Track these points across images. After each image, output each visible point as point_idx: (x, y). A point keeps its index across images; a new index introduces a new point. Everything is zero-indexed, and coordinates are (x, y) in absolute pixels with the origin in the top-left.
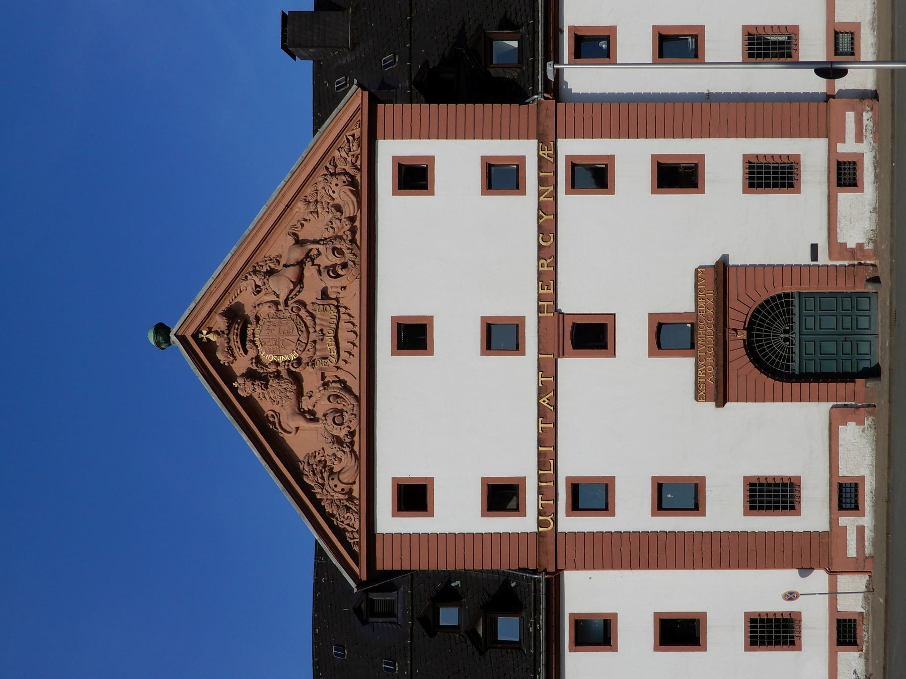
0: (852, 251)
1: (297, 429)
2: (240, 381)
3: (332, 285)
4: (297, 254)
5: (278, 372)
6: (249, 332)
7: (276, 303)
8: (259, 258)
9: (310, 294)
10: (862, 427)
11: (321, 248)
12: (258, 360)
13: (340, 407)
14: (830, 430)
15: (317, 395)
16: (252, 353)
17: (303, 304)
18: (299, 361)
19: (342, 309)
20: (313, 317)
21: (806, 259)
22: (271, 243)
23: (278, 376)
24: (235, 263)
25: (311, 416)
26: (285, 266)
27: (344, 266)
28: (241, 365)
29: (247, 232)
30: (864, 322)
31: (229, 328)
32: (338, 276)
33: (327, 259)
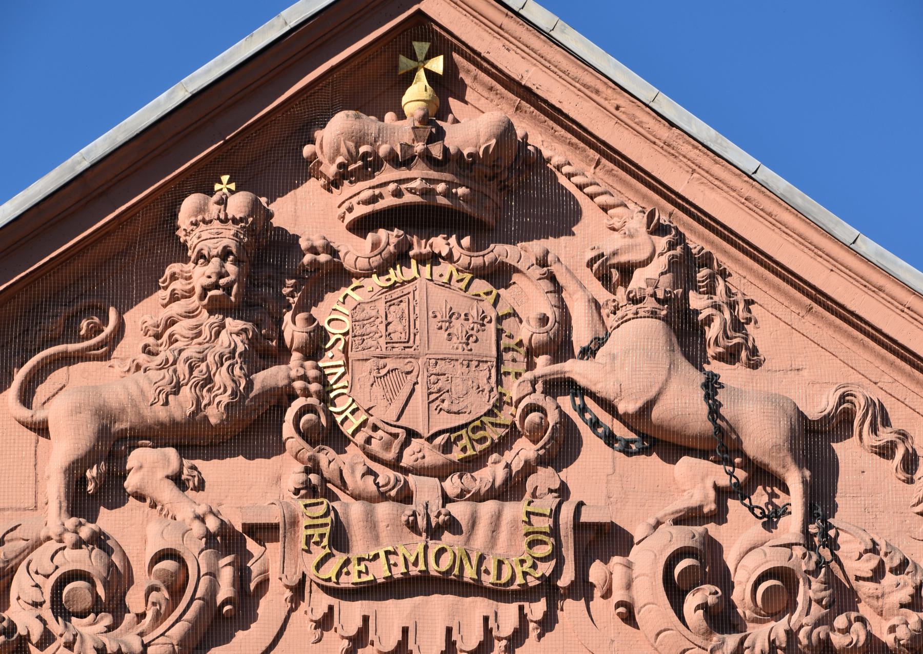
1: (41, 429)
2: (238, 204)
3: (640, 571)
4: (762, 435)
5: (281, 354)
6: (439, 244)
7: (560, 347)
8: (744, 279)
9: (602, 481)
11: (791, 526)
12: (335, 275)
13: (135, 599)
15: (185, 507)
16: (356, 251)
17: (562, 449)
18: (331, 436)
19: (537, 609)
20: (511, 488)
22: (808, 324)
23: (265, 350)
24: (719, 184)
25: (95, 484)
26: (711, 386)
27: (722, 618)
28: (311, 214)
29: (846, 232)
31: (451, 162)
32: (675, 593)
33: (749, 547)
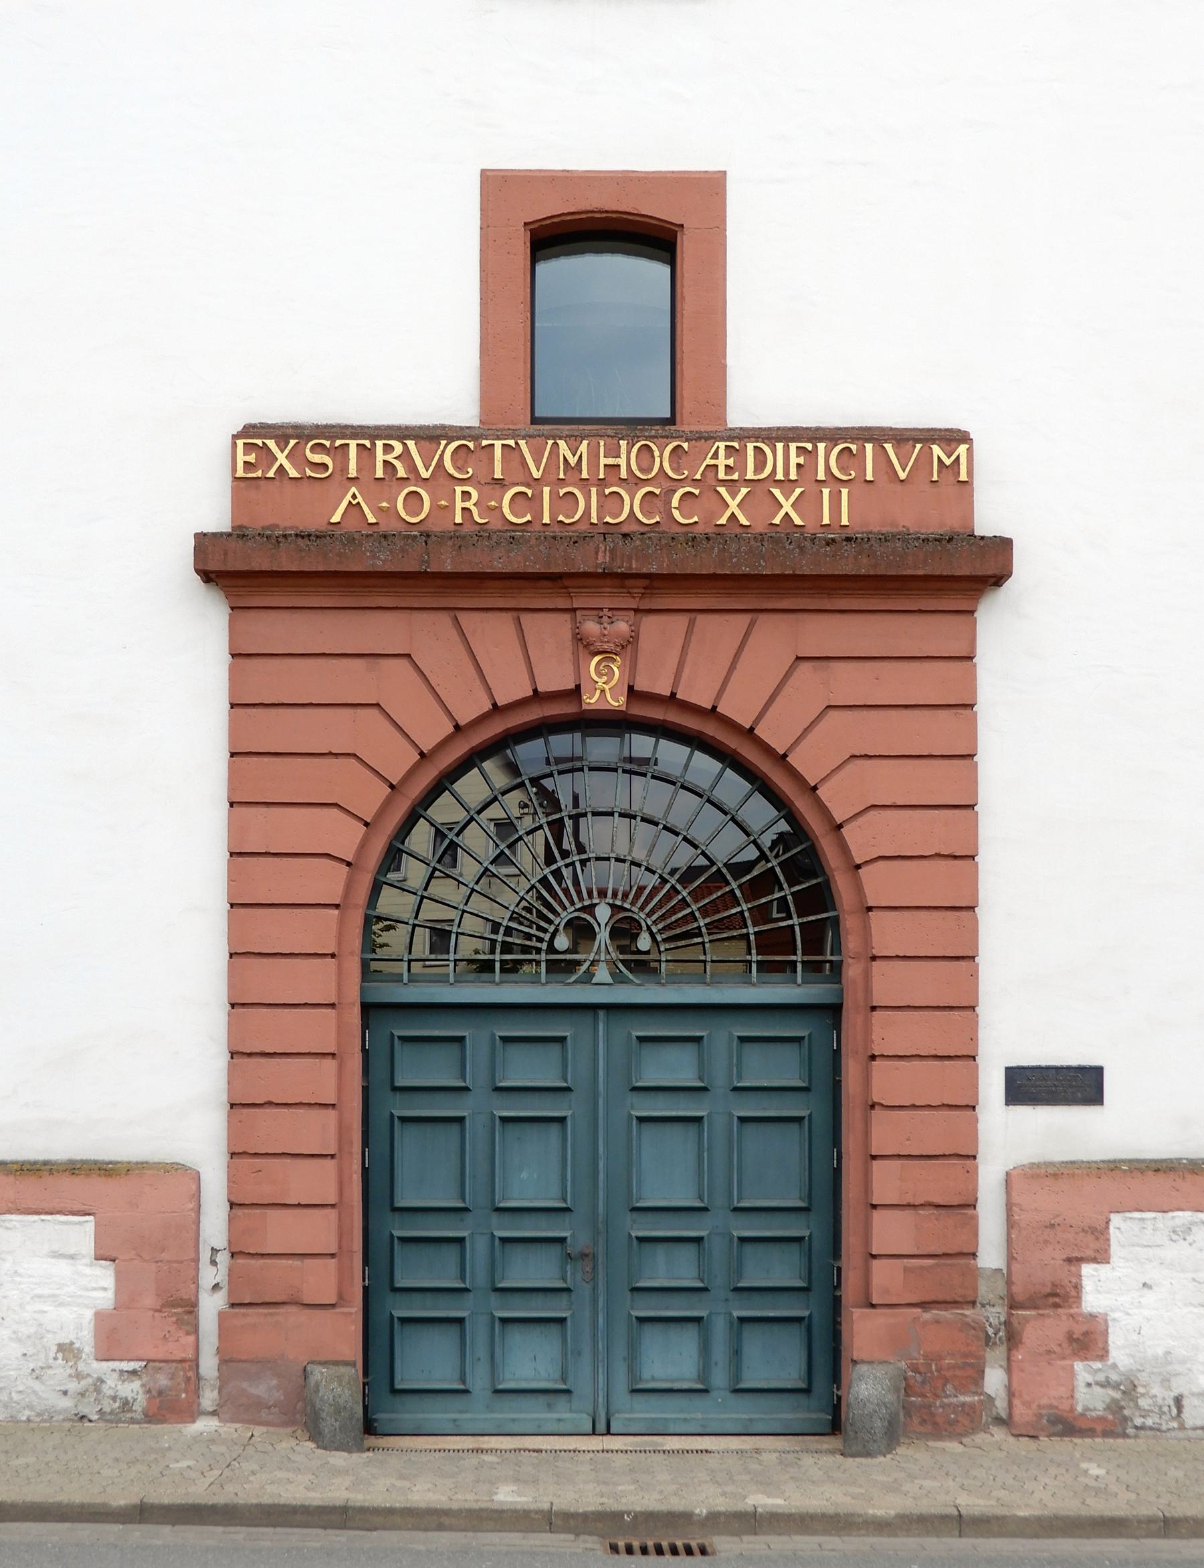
0: (1060, 1296)
10: (86, 1339)
14: (75, 1168)
21: (1011, 1033)
30: (671, 1359)
